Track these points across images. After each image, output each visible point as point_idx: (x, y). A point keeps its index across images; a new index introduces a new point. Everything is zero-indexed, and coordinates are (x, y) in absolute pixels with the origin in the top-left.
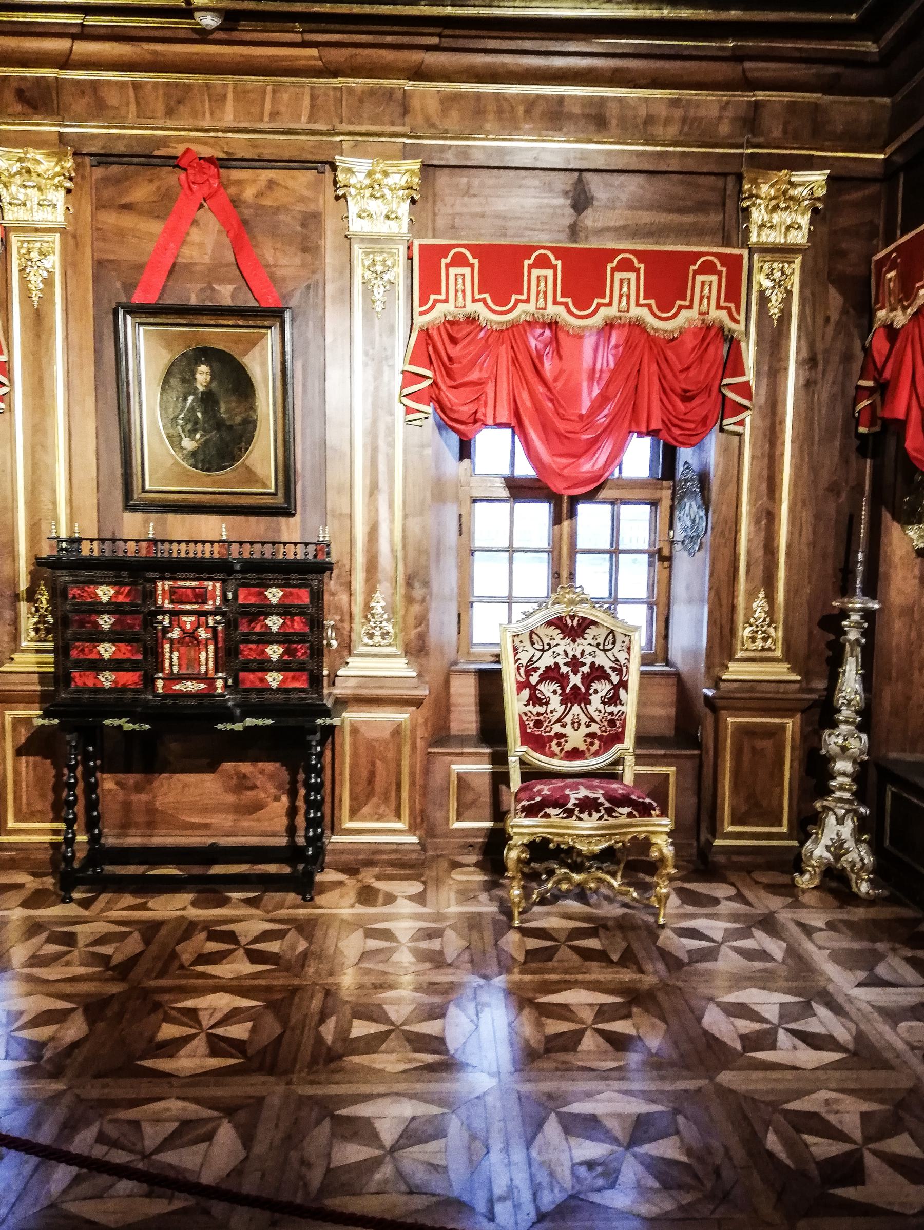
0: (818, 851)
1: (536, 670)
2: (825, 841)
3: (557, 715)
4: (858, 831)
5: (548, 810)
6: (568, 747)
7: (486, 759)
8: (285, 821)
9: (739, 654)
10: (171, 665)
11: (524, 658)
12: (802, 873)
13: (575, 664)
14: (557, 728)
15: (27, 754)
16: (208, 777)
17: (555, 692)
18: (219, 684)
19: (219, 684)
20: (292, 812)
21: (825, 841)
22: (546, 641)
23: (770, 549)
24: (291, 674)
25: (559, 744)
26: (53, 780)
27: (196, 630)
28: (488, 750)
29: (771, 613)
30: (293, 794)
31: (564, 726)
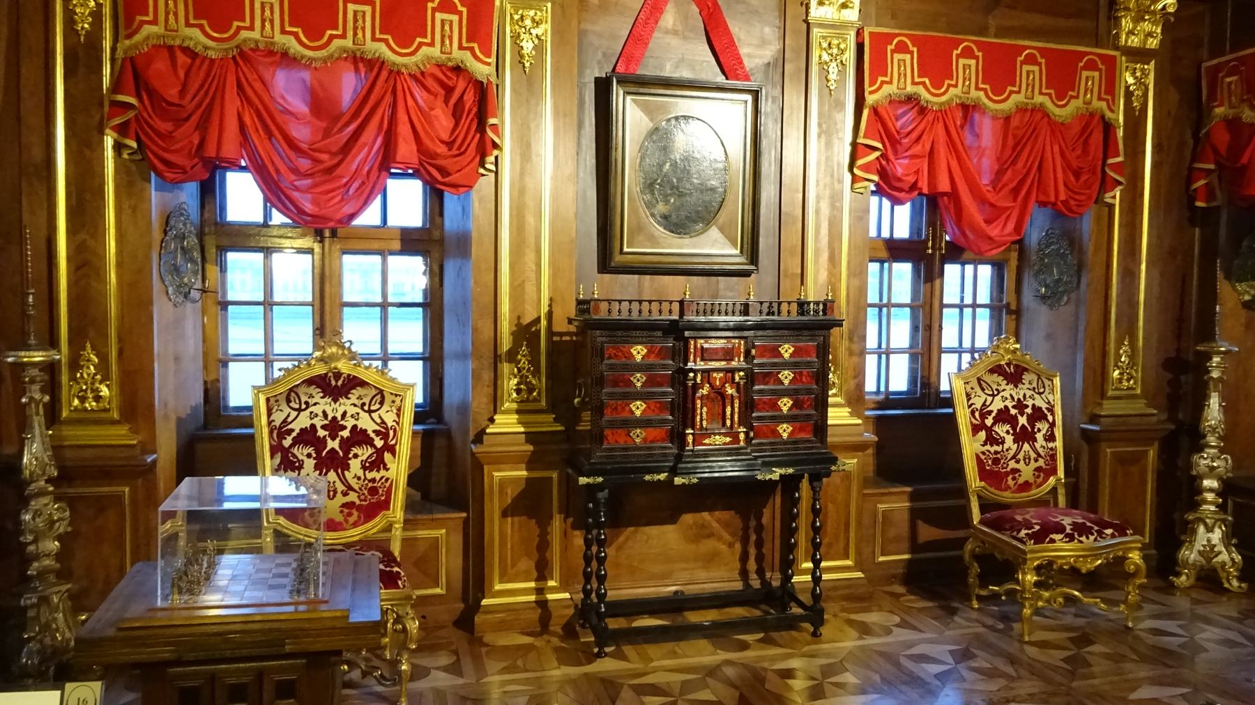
0: (1190, 554)
1: (990, 413)
2: (1198, 546)
3: (1012, 453)
4: (1226, 540)
5: (1054, 536)
6: (1021, 481)
7: (906, 497)
8: (738, 565)
9: (1110, 393)
10: (701, 420)
11: (978, 403)
12: (1178, 575)
13: (1020, 406)
14: (1012, 464)
15: (512, 516)
16: (669, 528)
17: (1008, 432)
18: (742, 436)
19: (742, 436)
20: (744, 558)
21: (1198, 546)
22: (995, 387)
23: (1133, 304)
24: (798, 425)
25: (1014, 479)
26: (537, 539)
27: (723, 386)
28: (909, 489)
29: (1132, 357)
30: (745, 541)
31: (1018, 462)
